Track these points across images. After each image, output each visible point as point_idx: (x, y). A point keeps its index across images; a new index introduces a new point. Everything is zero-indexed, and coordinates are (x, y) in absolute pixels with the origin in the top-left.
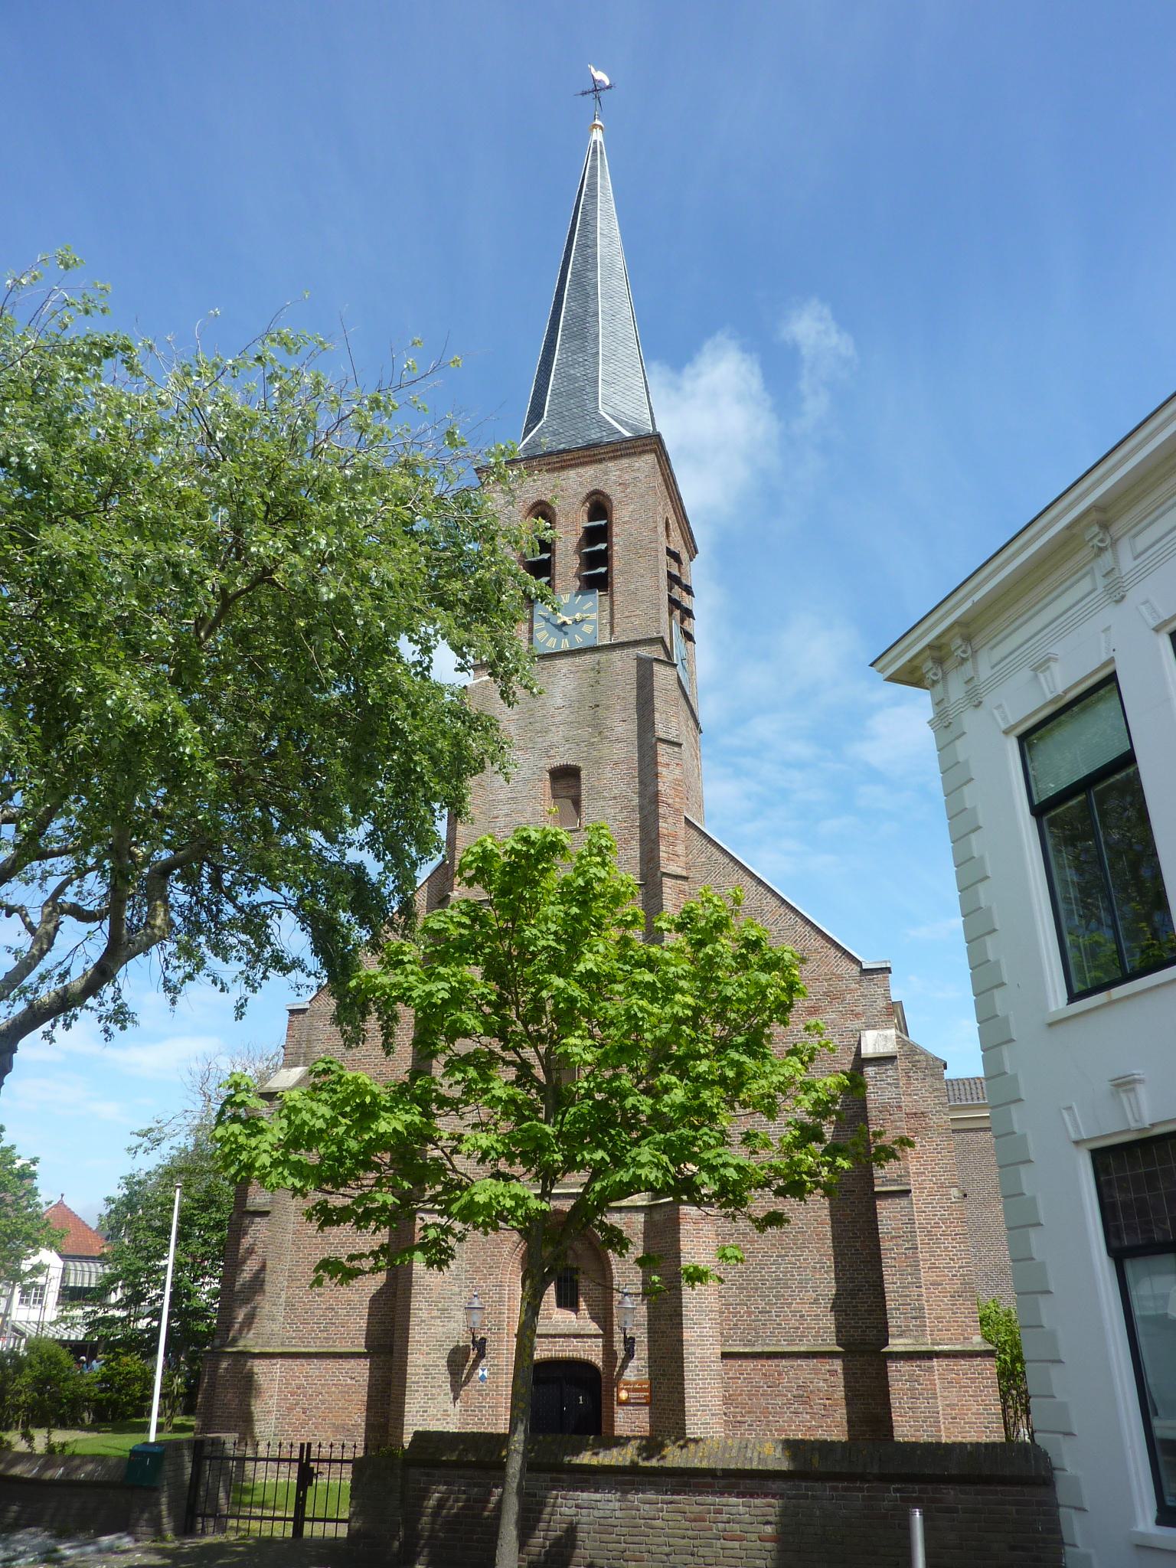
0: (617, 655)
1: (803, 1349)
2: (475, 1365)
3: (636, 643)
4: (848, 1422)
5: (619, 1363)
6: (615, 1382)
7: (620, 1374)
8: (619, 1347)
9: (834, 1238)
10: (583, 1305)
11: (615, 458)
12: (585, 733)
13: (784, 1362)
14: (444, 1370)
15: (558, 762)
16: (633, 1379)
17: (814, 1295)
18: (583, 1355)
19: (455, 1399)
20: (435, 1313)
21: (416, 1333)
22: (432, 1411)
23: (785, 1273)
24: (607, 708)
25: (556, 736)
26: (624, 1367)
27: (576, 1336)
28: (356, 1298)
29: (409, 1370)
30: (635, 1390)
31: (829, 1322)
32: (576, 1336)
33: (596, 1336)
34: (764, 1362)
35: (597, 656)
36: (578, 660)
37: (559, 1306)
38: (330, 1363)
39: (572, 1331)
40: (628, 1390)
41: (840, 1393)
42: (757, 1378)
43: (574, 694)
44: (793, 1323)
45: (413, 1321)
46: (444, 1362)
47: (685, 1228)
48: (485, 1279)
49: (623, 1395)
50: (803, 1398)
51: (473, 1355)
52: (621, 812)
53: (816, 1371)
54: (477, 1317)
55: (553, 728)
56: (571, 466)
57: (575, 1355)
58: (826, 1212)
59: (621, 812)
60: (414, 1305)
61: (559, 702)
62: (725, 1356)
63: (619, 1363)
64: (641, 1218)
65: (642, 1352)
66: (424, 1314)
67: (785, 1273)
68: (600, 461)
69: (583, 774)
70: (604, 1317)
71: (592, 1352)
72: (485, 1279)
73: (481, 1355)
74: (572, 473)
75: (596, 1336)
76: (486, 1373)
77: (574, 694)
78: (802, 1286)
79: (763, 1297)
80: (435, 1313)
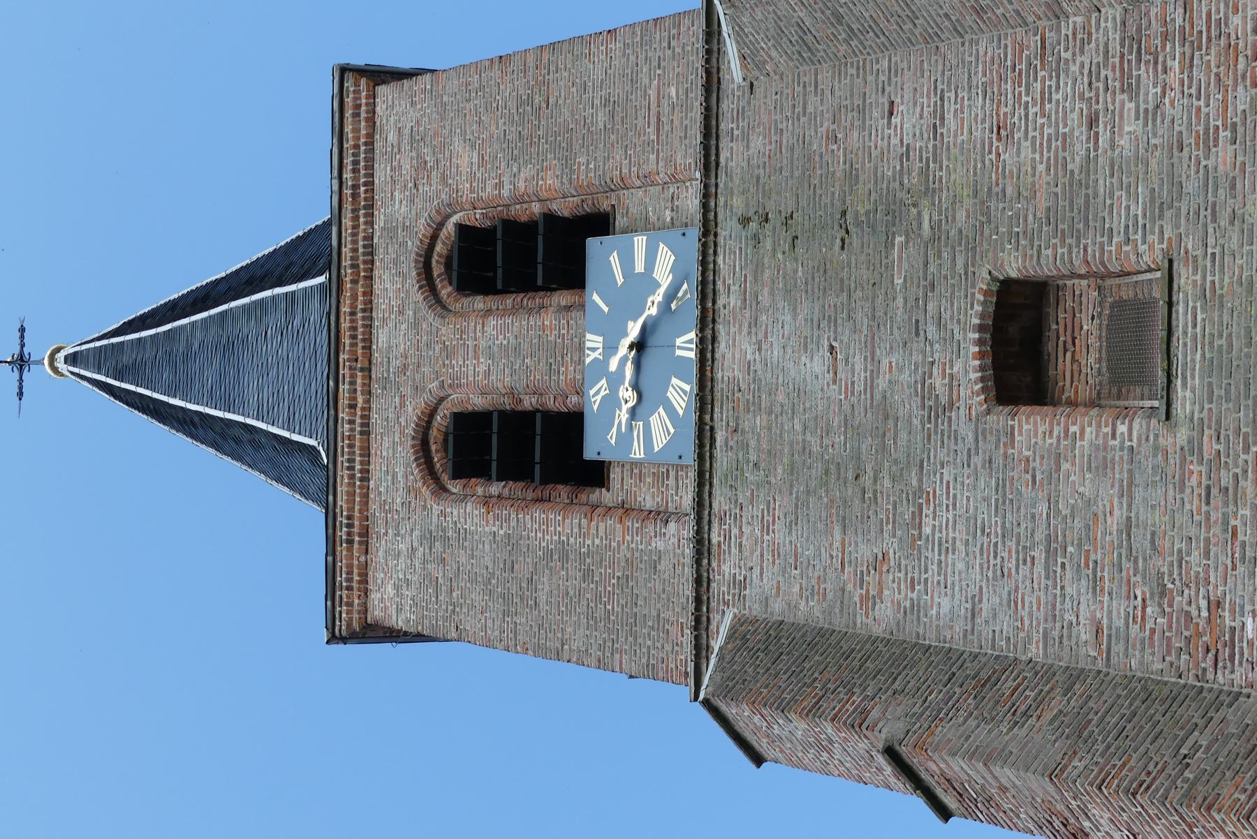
0: (731, 153)
3: (712, 83)
11: (370, 206)
12: (903, 258)
15: (966, 367)
24: (852, 176)
25: (896, 370)
35: (728, 229)
36: (728, 301)
43: (804, 310)
52: (1131, 89)
55: (882, 383)
56: (368, 348)
59: (1131, 89)
61: (817, 364)
68: (370, 250)
69: (1013, 268)
74: (381, 338)
77: (804, 310)
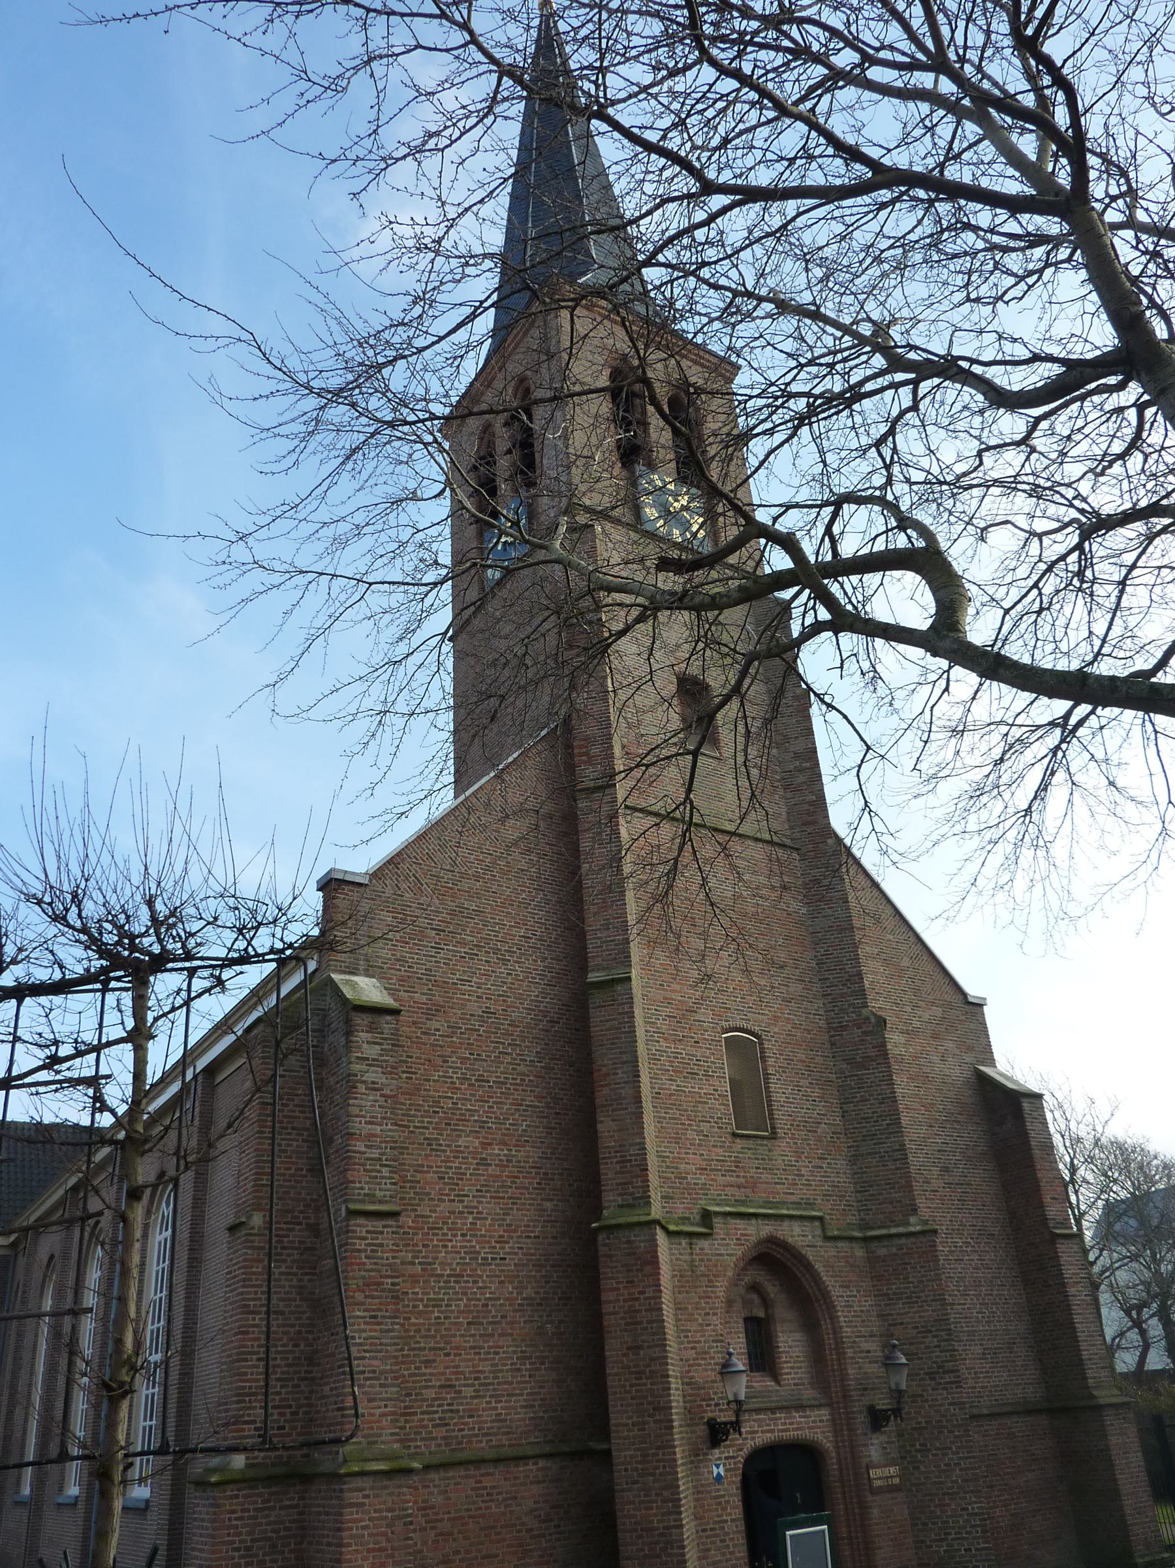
18: (806, 1434)
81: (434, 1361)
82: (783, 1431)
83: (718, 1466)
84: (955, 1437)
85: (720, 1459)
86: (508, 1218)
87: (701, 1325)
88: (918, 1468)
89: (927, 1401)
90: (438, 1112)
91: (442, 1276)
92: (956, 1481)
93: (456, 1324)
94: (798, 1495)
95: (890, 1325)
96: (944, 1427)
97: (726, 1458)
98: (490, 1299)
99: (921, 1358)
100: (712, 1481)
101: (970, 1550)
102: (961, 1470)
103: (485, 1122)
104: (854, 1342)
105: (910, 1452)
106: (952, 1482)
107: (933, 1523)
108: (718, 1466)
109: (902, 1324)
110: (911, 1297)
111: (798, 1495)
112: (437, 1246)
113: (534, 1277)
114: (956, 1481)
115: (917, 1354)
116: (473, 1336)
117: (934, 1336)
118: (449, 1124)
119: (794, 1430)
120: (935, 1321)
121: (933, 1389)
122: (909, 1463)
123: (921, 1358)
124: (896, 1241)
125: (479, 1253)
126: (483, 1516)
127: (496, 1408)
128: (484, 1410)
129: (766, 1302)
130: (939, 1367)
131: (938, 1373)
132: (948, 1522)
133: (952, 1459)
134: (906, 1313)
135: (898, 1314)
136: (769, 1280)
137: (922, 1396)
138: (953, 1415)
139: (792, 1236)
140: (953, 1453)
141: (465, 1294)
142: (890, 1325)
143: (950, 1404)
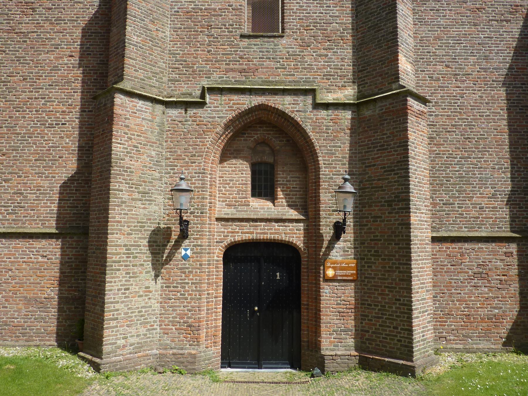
1: (484, 234)
2: (178, 245)
4: (521, 294)
5: (325, 244)
6: (318, 261)
7: (327, 254)
8: (327, 232)
9: (511, 144)
10: (280, 194)
13: (466, 245)
14: (145, 249)
16: (340, 259)
17: (493, 191)
18: (284, 238)
19: (156, 276)
20: (136, 196)
21: (116, 214)
22: (133, 288)
23: (467, 172)
26: (330, 247)
27: (277, 221)
28: (46, 184)
29: (110, 250)
30: (342, 269)
31: (504, 213)
32: (277, 221)
33: (297, 221)
34: (448, 245)
37: (253, 195)
38: (20, 243)
39: (273, 217)
40: (335, 269)
41: (514, 271)
42: (442, 257)
44: (474, 213)
45: (113, 201)
46: (145, 242)
47: (411, 119)
48: (187, 166)
49: (330, 273)
50: (483, 274)
51: (174, 236)
53: (494, 253)
54: (184, 199)
57: (276, 237)
58: (505, 122)
60: (114, 185)
62: (434, 240)
63: (325, 244)
64: (348, 115)
65: (349, 235)
66: (125, 196)
67: (467, 172)
70: (308, 204)
71: (295, 235)
72: (187, 166)
73: (184, 235)
75: (297, 221)
76: (189, 252)
78: (483, 183)
79: (447, 191)
80: (136, 196)
81: (11, 179)
82: (261, 233)
83: (186, 250)
84: (399, 248)
85: (190, 246)
86: (70, 101)
87: (187, 163)
88: (371, 267)
89: (383, 221)
90: (25, 41)
91: (20, 134)
92: (395, 280)
93: (26, 160)
94: (278, 274)
95: (366, 167)
96: (393, 240)
97: (194, 246)
98: (53, 147)
99: (384, 190)
100: (180, 258)
101: (397, 329)
102: (400, 272)
103: (59, 45)
104: (332, 178)
105: (366, 255)
106: (392, 279)
107: (375, 305)
108: (186, 250)
109: (374, 165)
110: (383, 145)
111: (278, 274)
112: (19, 117)
113: (86, 134)
114: (395, 280)
115: (382, 187)
116: (39, 167)
117: (395, 174)
118: (33, 48)
119: (271, 234)
120: (398, 162)
121: (389, 213)
122: (366, 263)
123: (384, 190)
124: (379, 104)
125: (47, 121)
126: (33, 262)
127: (51, 207)
128: (42, 207)
129: (273, 152)
130: (395, 197)
131: (395, 201)
132: (384, 306)
133: (395, 264)
134: (379, 157)
135: (373, 159)
136: (276, 138)
137: (381, 217)
138: (401, 232)
139: (283, 105)
140: (396, 260)
141: (35, 144)
142: (366, 167)
143: (399, 224)
